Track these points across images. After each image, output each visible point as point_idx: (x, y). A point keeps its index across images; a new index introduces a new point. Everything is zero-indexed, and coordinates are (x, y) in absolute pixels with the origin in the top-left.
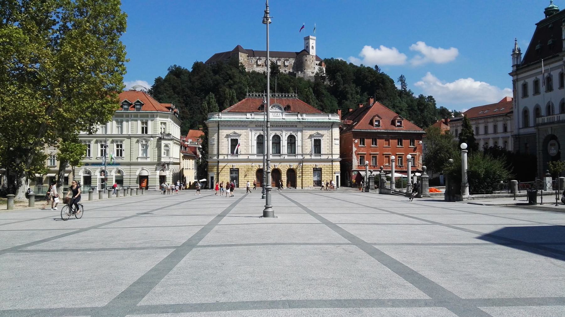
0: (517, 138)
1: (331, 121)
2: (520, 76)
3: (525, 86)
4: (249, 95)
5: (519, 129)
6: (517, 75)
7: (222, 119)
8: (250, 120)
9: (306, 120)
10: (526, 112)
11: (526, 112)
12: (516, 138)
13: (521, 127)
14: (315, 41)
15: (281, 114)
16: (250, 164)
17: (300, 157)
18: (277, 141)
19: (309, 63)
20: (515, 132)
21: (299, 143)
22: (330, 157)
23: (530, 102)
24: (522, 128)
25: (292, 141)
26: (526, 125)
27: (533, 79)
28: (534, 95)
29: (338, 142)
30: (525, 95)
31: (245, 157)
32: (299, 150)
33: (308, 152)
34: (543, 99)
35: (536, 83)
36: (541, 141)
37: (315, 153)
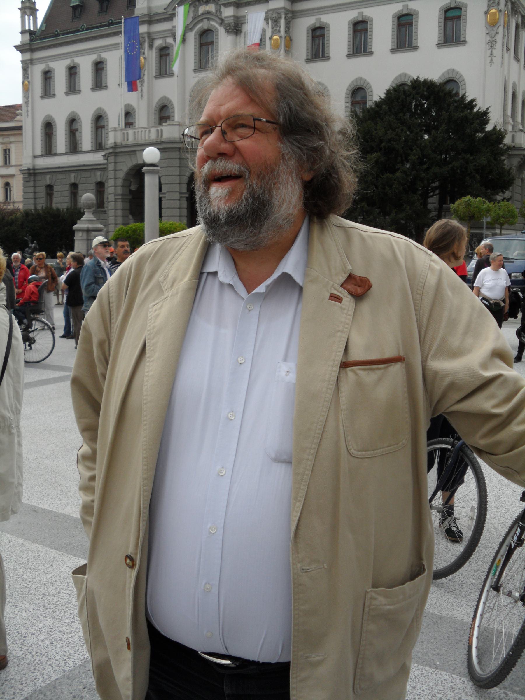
0: (32, 174)
2: (38, 55)
3: (47, 75)
5: (35, 157)
6: (32, 50)
10: (49, 127)
11: (49, 127)
12: (30, 174)
13: (38, 152)
20: (27, 162)
23: (59, 108)
24: (42, 156)
26: (49, 149)
27: (67, 62)
28: (67, 94)
30: (48, 92)
34: (85, 104)
35: (73, 71)
36: (121, 175)
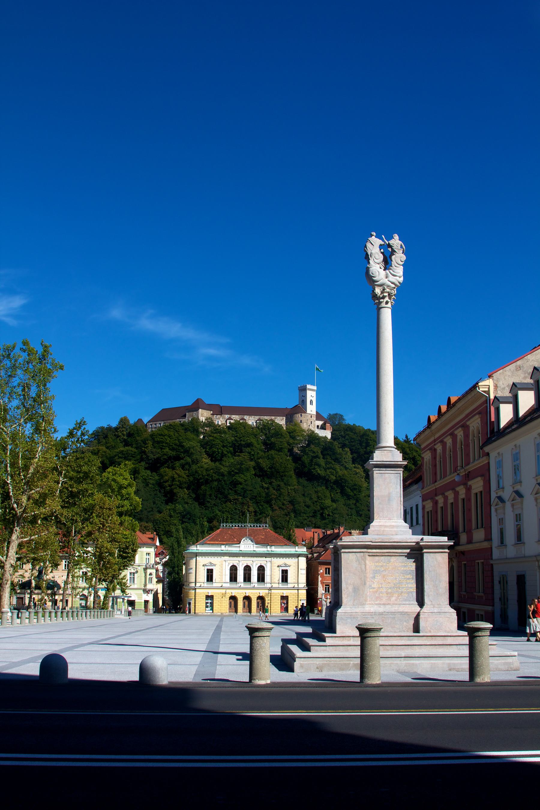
1: (298, 553)
4: (223, 526)
7: (200, 551)
8: (224, 552)
14: (314, 394)
15: (252, 546)
16: (223, 591)
17: (269, 586)
18: (247, 569)
21: (267, 573)
22: (296, 586)
25: (261, 569)
29: (304, 572)
31: (220, 585)
32: (267, 578)
33: (276, 580)
37: (282, 581)
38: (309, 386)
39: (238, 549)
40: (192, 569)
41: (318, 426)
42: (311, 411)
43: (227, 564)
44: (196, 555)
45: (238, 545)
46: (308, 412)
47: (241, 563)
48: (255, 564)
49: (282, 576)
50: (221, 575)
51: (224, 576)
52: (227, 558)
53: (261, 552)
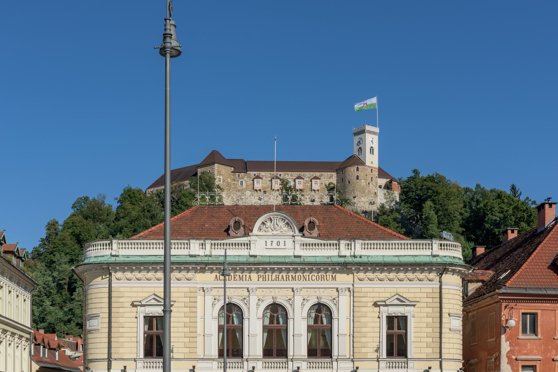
8: (198, 259)
9: (364, 260)
15: (289, 242)
19: (363, 182)
21: (341, 326)
29: (457, 324)
38: (368, 128)
39: (244, 252)
40: (96, 316)
41: (380, 187)
42: (372, 163)
43: (209, 299)
44: (106, 269)
45: (245, 240)
46: (367, 164)
47: (255, 297)
48: (300, 298)
49: (389, 337)
50: (192, 335)
51: (200, 340)
52: (208, 278)
53: (318, 260)
